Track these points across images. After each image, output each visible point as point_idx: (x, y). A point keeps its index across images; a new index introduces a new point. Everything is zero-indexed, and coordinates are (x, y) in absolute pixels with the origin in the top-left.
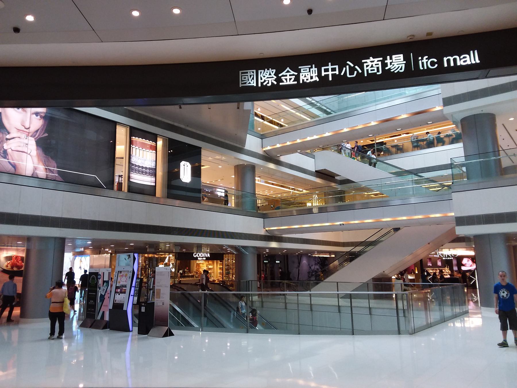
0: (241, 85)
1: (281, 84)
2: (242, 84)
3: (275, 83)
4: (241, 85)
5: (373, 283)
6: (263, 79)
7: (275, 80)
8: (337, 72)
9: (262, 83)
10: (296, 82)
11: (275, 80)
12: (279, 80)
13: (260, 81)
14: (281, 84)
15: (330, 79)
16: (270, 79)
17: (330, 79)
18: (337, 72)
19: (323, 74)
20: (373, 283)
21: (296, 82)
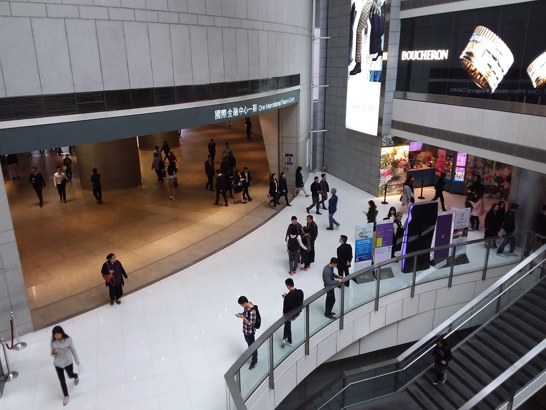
0: (216, 119)
1: (228, 117)
2: (216, 118)
3: (226, 117)
4: (216, 119)
5: (321, 39)
6: (223, 114)
7: (226, 115)
8: (243, 111)
9: (222, 117)
10: (232, 116)
11: (226, 115)
12: (227, 115)
13: (222, 116)
14: (228, 117)
15: (241, 115)
16: (225, 115)
17: (241, 115)
18: (243, 111)
19: (240, 112)
20: (321, 39)
21: (232, 116)
